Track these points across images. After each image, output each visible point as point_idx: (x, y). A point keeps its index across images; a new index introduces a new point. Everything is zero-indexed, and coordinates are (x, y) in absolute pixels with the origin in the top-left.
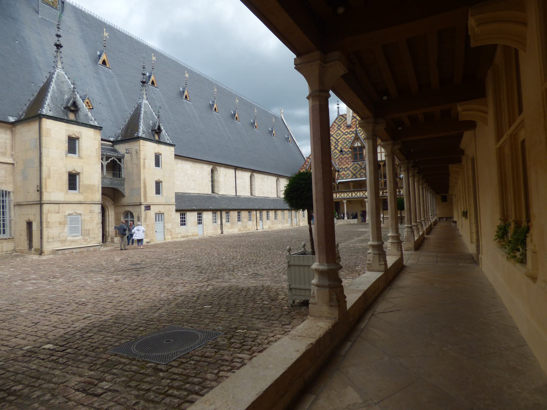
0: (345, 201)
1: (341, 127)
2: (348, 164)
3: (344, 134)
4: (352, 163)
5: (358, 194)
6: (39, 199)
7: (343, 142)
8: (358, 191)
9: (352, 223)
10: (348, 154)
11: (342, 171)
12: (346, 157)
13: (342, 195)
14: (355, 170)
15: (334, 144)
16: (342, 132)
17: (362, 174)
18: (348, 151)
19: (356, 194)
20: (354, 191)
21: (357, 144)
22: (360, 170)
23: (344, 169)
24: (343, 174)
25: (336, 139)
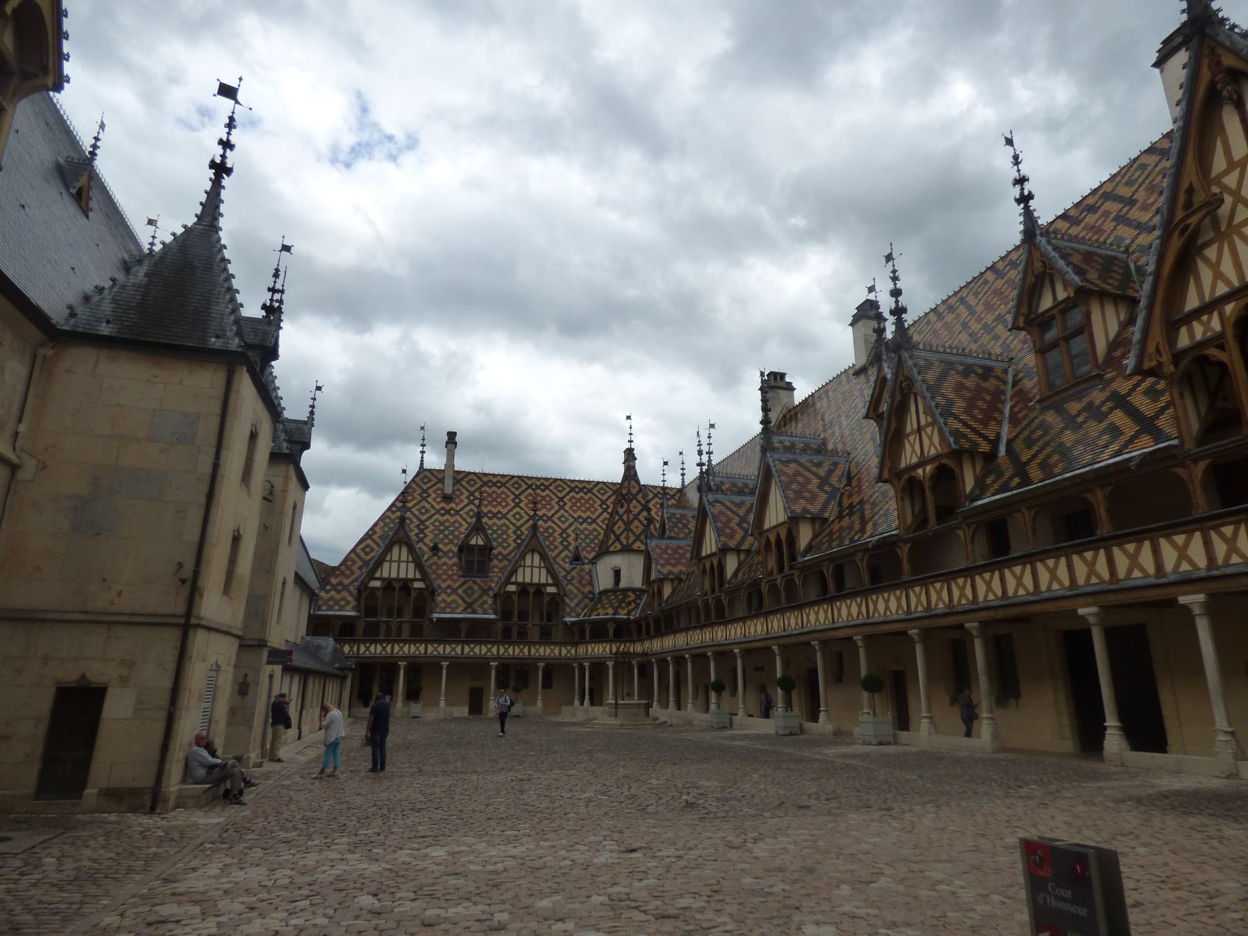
0: (445, 664)
1: (429, 495)
3: (438, 512)
4: (462, 580)
5: (477, 650)
6: (181, 609)
8: (477, 643)
9: (456, 714)
10: (450, 558)
12: (445, 564)
13: (441, 649)
14: (470, 596)
15: (417, 531)
17: (485, 606)
19: (472, 650)
20: (468, 643)
21: (477, 541)
22: (480, 597)
24: (444, 601)
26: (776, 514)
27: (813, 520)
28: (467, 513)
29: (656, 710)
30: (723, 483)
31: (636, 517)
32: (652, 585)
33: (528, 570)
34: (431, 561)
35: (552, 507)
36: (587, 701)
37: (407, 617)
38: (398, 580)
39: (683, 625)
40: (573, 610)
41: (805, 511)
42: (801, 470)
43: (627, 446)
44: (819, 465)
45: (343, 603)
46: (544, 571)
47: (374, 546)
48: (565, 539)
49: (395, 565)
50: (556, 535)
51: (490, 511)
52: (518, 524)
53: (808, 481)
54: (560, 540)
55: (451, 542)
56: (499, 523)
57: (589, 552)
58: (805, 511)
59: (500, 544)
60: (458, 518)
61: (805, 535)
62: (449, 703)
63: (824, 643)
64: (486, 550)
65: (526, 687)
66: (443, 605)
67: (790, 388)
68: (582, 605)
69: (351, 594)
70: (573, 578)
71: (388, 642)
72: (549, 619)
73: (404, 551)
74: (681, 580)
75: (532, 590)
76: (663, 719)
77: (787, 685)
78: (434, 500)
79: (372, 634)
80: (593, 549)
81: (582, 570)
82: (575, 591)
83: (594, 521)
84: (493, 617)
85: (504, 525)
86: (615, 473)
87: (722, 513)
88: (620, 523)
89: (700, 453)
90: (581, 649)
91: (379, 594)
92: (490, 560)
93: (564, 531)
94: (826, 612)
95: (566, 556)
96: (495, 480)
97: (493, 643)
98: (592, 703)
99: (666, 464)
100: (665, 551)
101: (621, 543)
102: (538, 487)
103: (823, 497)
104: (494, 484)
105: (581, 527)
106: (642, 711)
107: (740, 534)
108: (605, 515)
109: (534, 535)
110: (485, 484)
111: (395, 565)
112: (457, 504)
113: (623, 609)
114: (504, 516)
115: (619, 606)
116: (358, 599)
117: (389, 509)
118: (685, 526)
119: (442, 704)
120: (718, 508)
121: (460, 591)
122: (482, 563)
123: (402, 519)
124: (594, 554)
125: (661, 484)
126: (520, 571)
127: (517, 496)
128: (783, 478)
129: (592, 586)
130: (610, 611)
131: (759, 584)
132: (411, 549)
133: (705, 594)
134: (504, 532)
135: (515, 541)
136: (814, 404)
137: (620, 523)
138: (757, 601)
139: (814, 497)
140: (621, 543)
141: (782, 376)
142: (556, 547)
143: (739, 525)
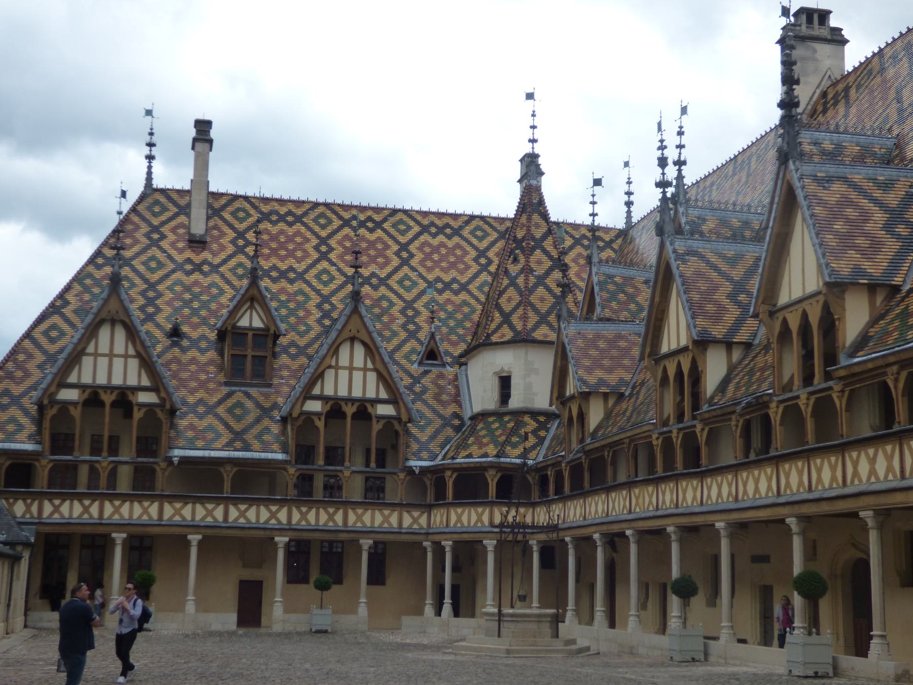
0: (195, 538)
1: (163, 237)
2: (207, 390)
3: (179, 267)
4: (225, 390)
5: (251, 514)
7: (178, 297)
8: (251, 502)
9: (216, 627)
10: (202, 351)
11: (185, 414)
12: (193, 360)
13: (187, 512)
14: (239, 419)
15: (141, 301)
16: (170, 257)
17: (266, 437)
18: (203, 337)
19: (242, 514)
20: (236, 501)
21: (251, 320)
22: (258, 420)
23: (193, 409)
24: (192, 427)
25: (146, 281)
26: (802, 277)
27: (872, 288)
28: (233, 270)
29: (570, 626)
30: (704, 220)
31: (541, 280)
32: (567, 405)
33: (343, 375)
34: (169, 356)
35: (388, 262)
36: (447, 608)
37: (127, 454)
38: (109, 388)
39: (622, 478)
40: (423, 447)
41: (858, 271)
42: (853, 195)
43: (527, 149)
44: (887, 186)
45: (11, 427)
46: (372, 377)
47: (65, 327)
48: (410, 320)
49: (103, 362)
50: (395, 311)
51: (274, 268)
52: (326, 291)
53: (866, 217)
54: (401, 320)
55: (204, 322)
56: (291, 289)
57: (454, 344)
58: (858, 271)
59: (293, 328)
60: (216, 278)
61: (855, 318)
62: (203, 606)
63: (884, 514)
64: (268, 337)
65: (339, 581)
66: (190, 434)
67: (837, 39)
68: (440, 439)
69: (26, 412)
70: (425, 390)
71: (94, 497)
72: (381, 463)
73: (120, 335)
74: (621, 396)
75: (350, 410)
76: (582, 643)
77: (811, 587)
78: (173, 244)
79: (63, 482)
80: (462, 338)
81: (441, 376)
82: (429, 414)
83: (464, 287)
84: (280, 456)
85: (301, 292)
86: (504, 202)
87: (699, 274)
88: (511, 292)
89: (663, 162)
90: (438, 517)
91: (76, 413)
92: (275, 355)
93: (409, 304)
94: (889, 459)
95: (413, 351)
96: (283, 210)
97: (282, 502)
98: (456, 613)
99: (600, 182)
100: (592, 343)
101: (512, 327)
102: (362, 224)
103: (892, 246)
104: (282, 218)
105: (441, 299)
106: (546, 628)
107: (733, 313)
108: (485, 277)
109: (355, 311)
110: (265, 217)
111: (103, 362)
112: (214, 254)
113: (514, 446)
114: (301, 276)
115: (507, 442)
116: (39, 422)
117: (92, 261)
118: (631, 298)
119: (190, 607)
120: (693, 265)
121: (221, 410)
122: (260, 360)
123: (116, 280)
124: (463, 347)
125: (588, 221)
126: (329, 375)
127: (323, 241)
128: (818, 210)
129: (460, 406)
130: (492, 450)
131: (766, 405)
132: (132, 334)
133: (665, 423)
134: (300, 305)
135: (319, 321)
136: (882, 70)
137: (511, 292)
138: (760, 436)
139: (876, 246)
140: (512, 327)
141: (824, 15)
142: (395, 334)
143: (732, 297)
